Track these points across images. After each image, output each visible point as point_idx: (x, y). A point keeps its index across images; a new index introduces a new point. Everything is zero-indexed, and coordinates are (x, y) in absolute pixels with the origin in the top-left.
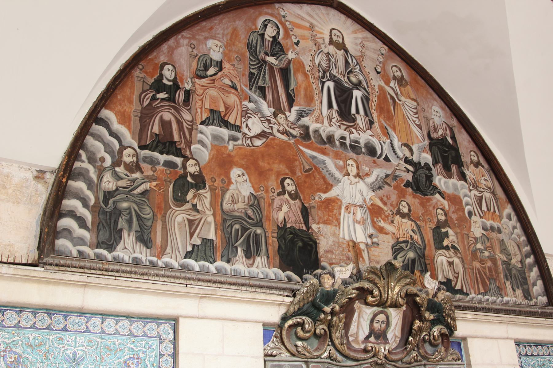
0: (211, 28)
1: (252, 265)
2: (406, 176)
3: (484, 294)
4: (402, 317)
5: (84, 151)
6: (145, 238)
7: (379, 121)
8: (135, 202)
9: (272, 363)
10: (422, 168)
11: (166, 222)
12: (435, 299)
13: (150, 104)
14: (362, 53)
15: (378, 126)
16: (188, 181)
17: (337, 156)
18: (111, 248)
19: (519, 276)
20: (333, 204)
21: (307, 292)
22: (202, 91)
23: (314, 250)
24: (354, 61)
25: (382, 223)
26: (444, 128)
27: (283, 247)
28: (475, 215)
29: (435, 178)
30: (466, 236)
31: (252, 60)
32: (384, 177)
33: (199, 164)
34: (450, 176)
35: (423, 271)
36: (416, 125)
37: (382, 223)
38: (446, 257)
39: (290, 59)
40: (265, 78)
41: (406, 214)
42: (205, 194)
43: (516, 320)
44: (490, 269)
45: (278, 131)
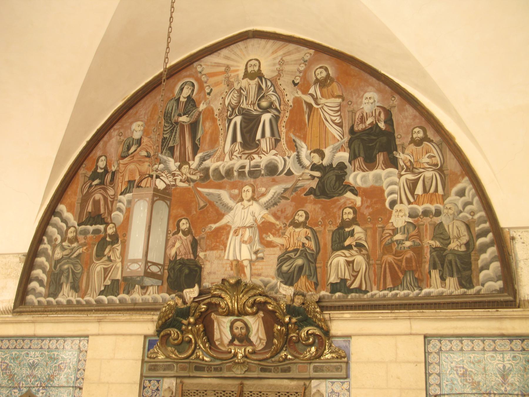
0: (137, 112)
1: (145, 293)
2: (309, 184)
3: (391, 290)
4: (262, 322)
5: (47, 237)
6: (76, 286)
7: (287, 136)
8: (72, 264)
9: (150, 364)
10: (334, 169)
11: (89, 273)
12: (294, 304)
13: (88, 191)
14: (279, 71)
15: (285, 143)
16: (107, 241)
17: (234, 186)
18: (55, 296)
19: (457, 260)
20: (222, 231)
21: (165, 311)
22: (124, 168)
23: (199, 273)
24: (269, 84)
25: (271, 238)
26: (377, 113)
27: (172, 276)
28: (401, 202)
29: (349, 175)
30: (381, 229)
31: (166, 127)
32: (282, 192)
33: (115, 226)
34: (371, 169)
35: (311, 276)
36: (336, 124)
37: (271, 238)
38: (346, 257)
39: (201, 110)
40: (175, 138)
41: (302, 222)
42: (117, 248)
43: (419, 314)
44: (408, 261)
45: (181, 181)
